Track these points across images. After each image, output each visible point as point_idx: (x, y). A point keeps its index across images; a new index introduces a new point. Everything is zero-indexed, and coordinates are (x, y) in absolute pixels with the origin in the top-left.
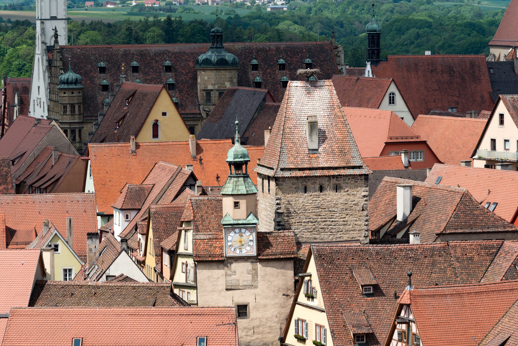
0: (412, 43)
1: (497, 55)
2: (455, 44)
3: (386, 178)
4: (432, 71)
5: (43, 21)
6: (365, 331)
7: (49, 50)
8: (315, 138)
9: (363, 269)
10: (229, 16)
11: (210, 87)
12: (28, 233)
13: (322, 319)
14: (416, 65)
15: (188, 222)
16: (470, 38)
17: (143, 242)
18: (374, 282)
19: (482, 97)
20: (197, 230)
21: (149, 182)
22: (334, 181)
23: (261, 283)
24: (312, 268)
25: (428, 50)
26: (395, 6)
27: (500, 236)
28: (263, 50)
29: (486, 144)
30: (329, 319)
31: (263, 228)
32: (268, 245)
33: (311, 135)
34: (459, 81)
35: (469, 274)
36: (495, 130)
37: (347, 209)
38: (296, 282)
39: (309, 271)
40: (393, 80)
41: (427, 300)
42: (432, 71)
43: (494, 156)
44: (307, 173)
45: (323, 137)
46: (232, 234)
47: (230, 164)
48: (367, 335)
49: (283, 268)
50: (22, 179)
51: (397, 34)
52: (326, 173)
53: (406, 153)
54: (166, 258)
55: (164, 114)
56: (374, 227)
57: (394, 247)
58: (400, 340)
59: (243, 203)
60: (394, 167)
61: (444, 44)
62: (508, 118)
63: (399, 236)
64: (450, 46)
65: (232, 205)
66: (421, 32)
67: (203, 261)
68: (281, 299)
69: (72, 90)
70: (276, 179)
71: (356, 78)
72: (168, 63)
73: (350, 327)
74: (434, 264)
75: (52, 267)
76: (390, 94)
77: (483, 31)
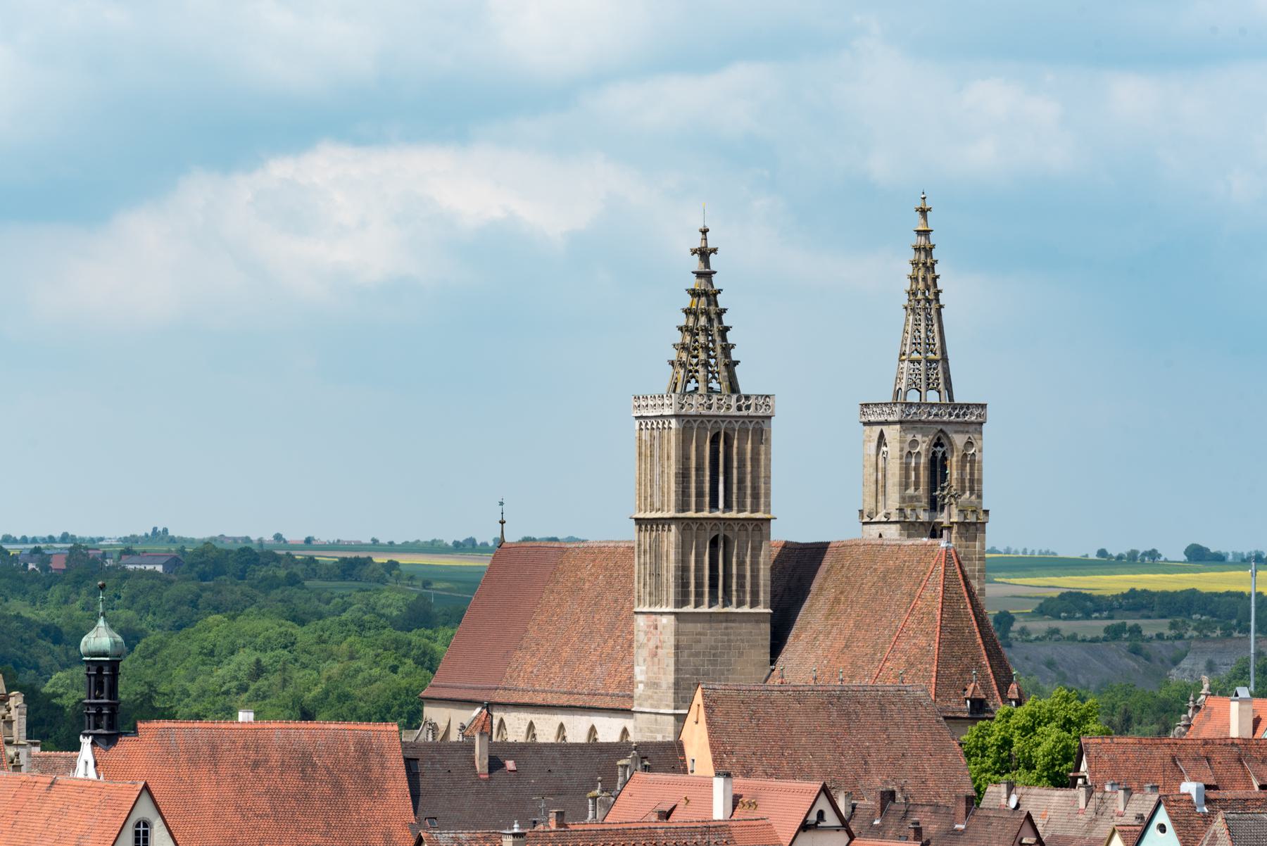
0: (243, 689)
1: (442, 726)
2: (358, 693)
4: (256, 764)
14: (214, 748)
16: (395, 676)
25: (246, 706)
26: (203, 590)
34: (327, 789)
40: (146, 787)
42: (256, 764)
51: (204, 664)
61: (327, 693)
66: (266, 659)
71: (50, 780)
76: (138, 825)
77: (431, 659)
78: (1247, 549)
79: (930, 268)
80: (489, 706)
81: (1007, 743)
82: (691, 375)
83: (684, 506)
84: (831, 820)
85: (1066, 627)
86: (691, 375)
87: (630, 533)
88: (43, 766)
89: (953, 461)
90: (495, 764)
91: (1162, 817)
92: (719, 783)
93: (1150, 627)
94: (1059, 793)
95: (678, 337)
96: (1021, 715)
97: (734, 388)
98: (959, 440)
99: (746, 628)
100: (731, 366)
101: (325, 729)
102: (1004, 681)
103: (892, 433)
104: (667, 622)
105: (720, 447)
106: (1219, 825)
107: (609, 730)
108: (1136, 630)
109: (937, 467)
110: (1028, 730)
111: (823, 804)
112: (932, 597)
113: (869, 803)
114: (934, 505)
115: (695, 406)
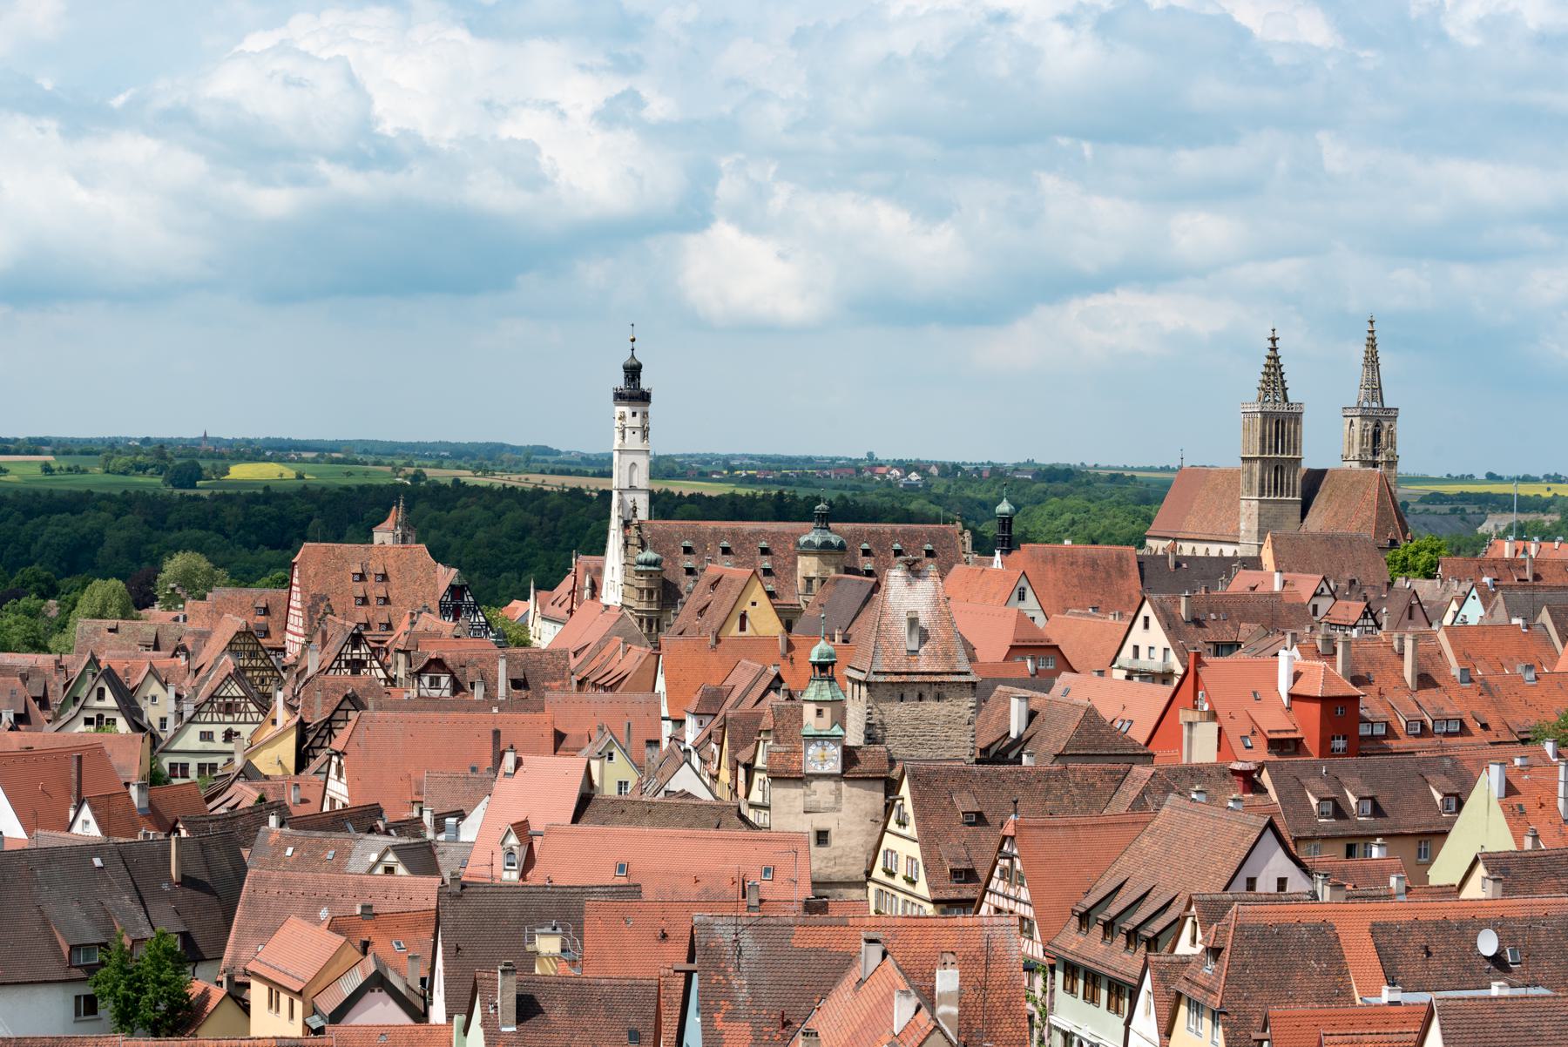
3: (1000, 687)
5: (621, 492)
6: (964, 866)
7: (626, 525)
8: (916, 638)
9: (965, 793)
10: (838, 492)
11: (812, 574)
12: (580, 737)
13: (915, 850)
15: (768, 731)
17: (717, 753)
18: (977, 809)
19: (1130, 596)
20: (777, 740)
21: (729, 682)
22: (935, 688)
23: (845, 806)
24: (905, 790)
27: (1129, 759)
28: (877, 533)
29: (1127, 652)
30: (922, 851)
31: (850, 742)
32: (855, 761)
33: (910, 633)
35: (1089, 803)
36: (1137, 635)
37: (950, 722)
38: (887, 805)
39: (901, 793)
41: (1035, 832)
43: (1137, 665)
44: (904, 678)
45: (924, 637)
46: (813, 747)
47: (814, 664)
48: (967, 871)
49: (872, 789)
50: (584, 674)
52: (927, 678)
53: (1033, 658)
54: (741, 771)
55: (754, 604)
56: (983, 745)
57: (1002, 768)
58: (1002, 878)
59: (827, 711)
60: (1017, 675)
62: (1154, 621)
63: (1012, 755)
64: (1110, 535)
65: (814, 712)
67: (779, 778)
68: (868, 825)
69: (650, 573)
70: (868, 684)
72: (764, 544)
73: (946, 861)
74: (1048, 790)
75: (602, 778)
78: (1513, 474)
79: (1374, 347)
80: (1176, 540)
81: (1406, 559)
82: (1267, 394)
83: (1263, 452)
84: (1327, 592)
85: (1432, 508)
86: (1267, 394)
87: (1240, 464)
88: (980, 563)
89: (1384, 433)
90: (1178, 565)
91: (1474, 592)
92: (1277, 575)
93: (1469, 509)
94: (1428, 582)
95: (1262, 377)
96: (1412, 547)
97: (1286, 400)
98: (1386, 424)
99: (1290, 507)
100: (1285, 390)
101: (1103, 548)
102: (1405, 531)
103: (1356, 421)
104: (1255, 503)
105: (1280, 426)
106: (1499, 597)
107: (1228, 551)
108: (1463, 510)
109: (1376, 436)
110: (1415, 554)
111: (1324, 585)
112: (1373, 494)
113: (1344, 584)
114: (1375, 453)
115: (1269, 408)
